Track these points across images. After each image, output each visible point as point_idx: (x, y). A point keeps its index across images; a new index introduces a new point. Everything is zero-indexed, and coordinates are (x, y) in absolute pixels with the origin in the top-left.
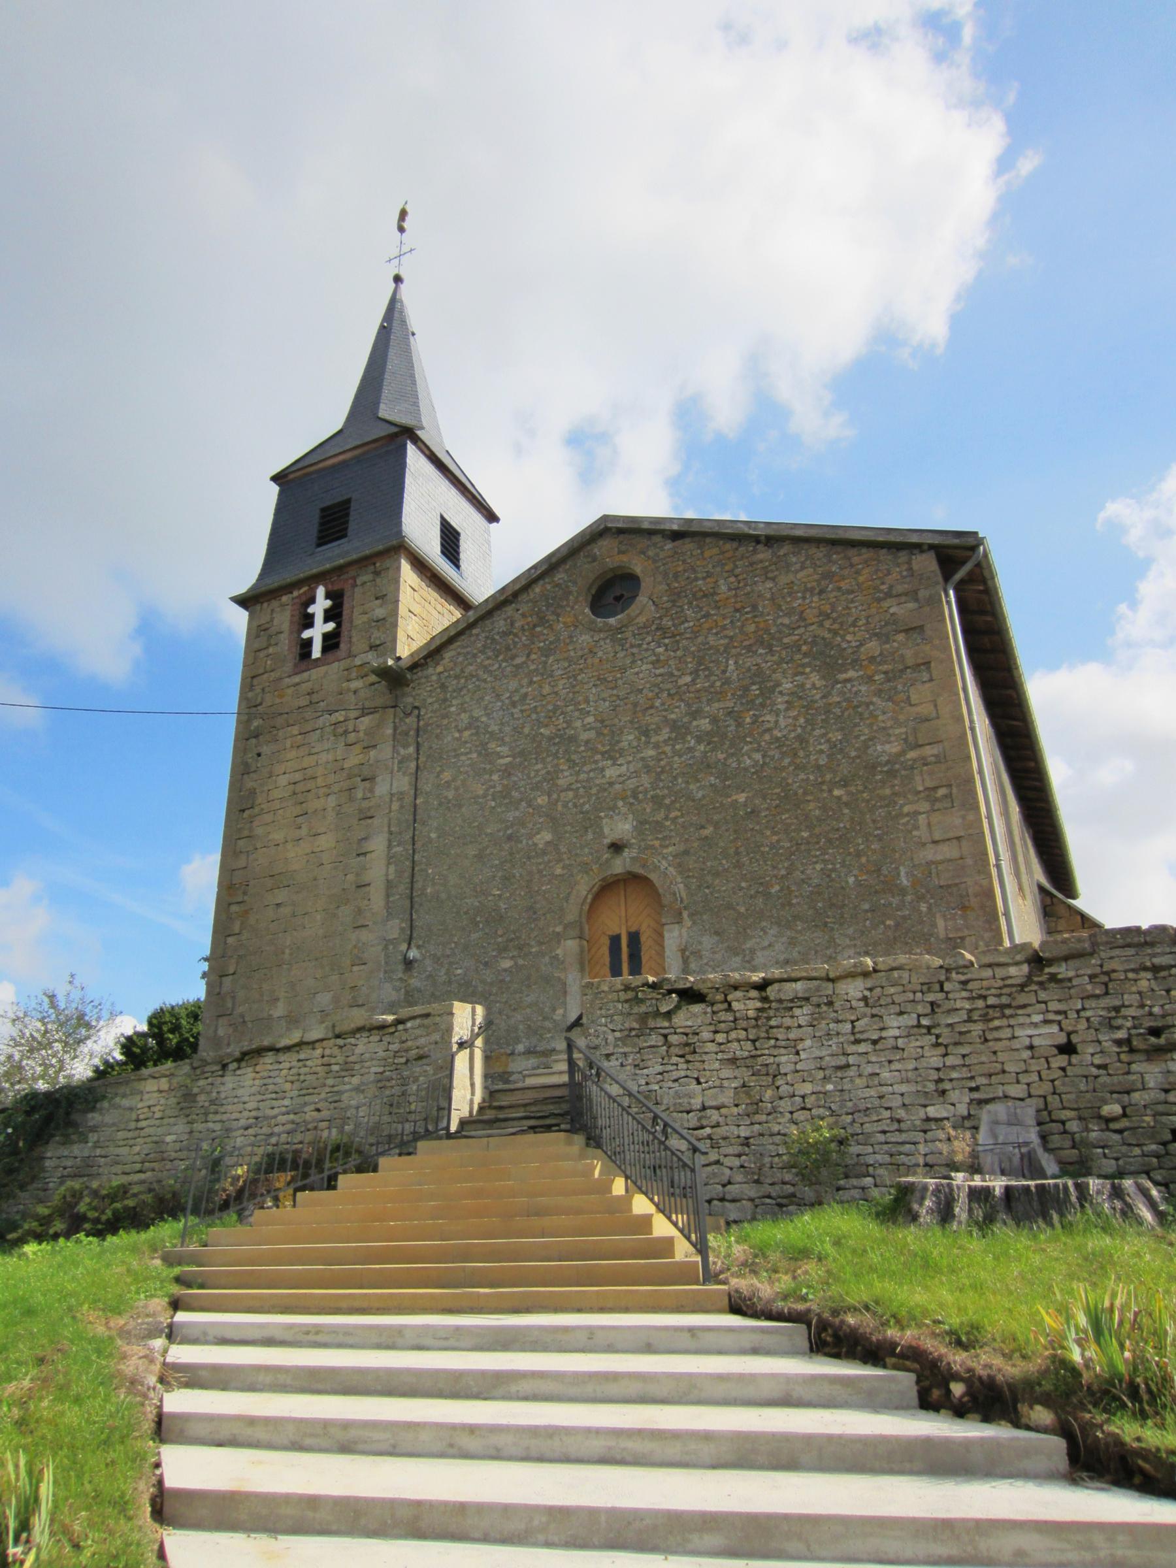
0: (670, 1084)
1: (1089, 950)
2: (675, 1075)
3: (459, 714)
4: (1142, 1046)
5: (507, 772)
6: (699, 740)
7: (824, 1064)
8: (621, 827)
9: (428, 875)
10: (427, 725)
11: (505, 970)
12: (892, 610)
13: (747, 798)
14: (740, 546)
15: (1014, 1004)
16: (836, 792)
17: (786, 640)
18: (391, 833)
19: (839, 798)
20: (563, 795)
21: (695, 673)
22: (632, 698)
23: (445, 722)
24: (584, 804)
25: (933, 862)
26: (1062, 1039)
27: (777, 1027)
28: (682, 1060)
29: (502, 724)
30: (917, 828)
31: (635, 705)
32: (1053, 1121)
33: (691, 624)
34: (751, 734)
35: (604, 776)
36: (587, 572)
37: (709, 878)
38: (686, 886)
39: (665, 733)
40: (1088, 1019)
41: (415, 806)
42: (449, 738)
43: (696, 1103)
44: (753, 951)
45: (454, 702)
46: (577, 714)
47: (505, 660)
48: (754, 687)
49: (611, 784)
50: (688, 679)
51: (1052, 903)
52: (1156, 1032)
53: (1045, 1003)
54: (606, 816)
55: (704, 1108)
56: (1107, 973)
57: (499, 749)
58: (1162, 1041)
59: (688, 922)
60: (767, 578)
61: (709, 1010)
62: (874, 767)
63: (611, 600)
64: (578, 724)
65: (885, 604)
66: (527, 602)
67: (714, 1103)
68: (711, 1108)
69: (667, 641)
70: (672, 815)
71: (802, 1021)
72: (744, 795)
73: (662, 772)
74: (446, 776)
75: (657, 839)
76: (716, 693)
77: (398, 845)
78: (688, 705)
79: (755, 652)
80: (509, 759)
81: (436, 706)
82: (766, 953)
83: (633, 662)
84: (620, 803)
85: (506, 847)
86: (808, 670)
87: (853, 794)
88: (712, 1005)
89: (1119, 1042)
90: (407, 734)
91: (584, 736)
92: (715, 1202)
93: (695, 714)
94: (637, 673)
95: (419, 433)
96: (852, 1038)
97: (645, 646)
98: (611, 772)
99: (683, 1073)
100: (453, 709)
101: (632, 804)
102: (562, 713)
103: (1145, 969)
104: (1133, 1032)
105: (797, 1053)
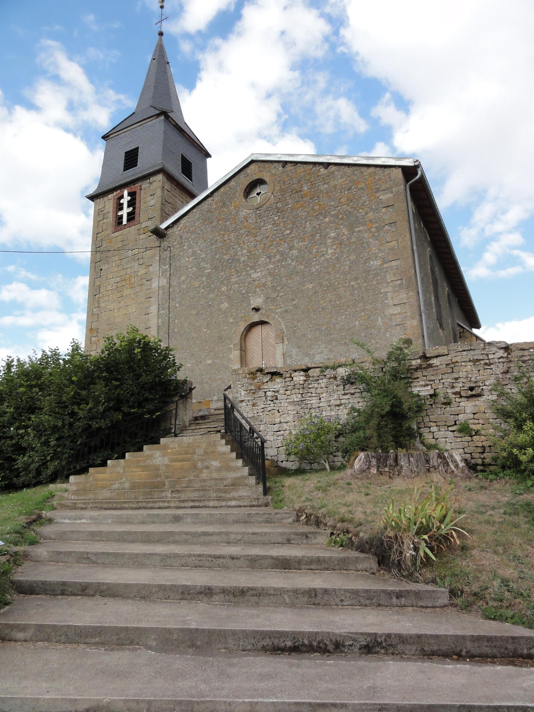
0: (267, 413)
1: (447, 353)
2: (269, 409)
3: (188, 250)
4: (465, 395)
5: (209, 275)
6: (293, 260)
7: (331, 404)
8: (257, 301)
9: (175, 323)
10: (174, 255)
11: (209, 364)
12: (380, 198)
13: (313, 286)
14: (313, 167)
15: (413, 377)
16: (352, 283)
17: (332, 213)
18: (159, 305)
19: (353, 286)
20: (233, 286)
21: (292, 229)
22: (264, 242)
23: (182, 253)
24: (242, 290)
25: (393, 314)
26: (432, 392)
27: (312, 388)
28: (272, 402)
29: (207, 254)
30: (387, 299)
31: (265, 244)
32: (425, 427)
33: (290, 206)
34: (315, 257)
35: (251, 277)
36: (244, 181)
37: (295, 323)
38: (286, 326)
39: (278, 257)
40: (443, 383)
41: (169, 291)
42: (184, 261)
43: (278, 420)
44: (314, 355)
45: (186, 244)
46: (239, 249)
47: (208, 224)
48: (317, 235)
49: (254, 281)
50: (288, 232)
51: (463, 332)
52: (471, 389)
53: (426, 376)
54: (252, 296)
55: (281, 423)
56: (453, 363)
57: (205, 266)
58: (474, 392)
59: (286, 342)
60: (325, 183)
61: (284, 381)
62: (369, 271)
63: (255, 195)
64: (240, 253)
65: (377, 195)
66: (219, 196)
67: (285, 421)
68: (284, 422)
69: (279, 214)
70: (281, 294)
71: (323, 385)
72: (312, 285)
73: (276, 275)
74: (183, 278)
75: (273, 305)
76: (301, 238)
77: (163, 310)
78: (288, 244)
79: (318, 219)
80: (210, 270)
81: (178, 246)
82: (319, 355)
83: (265, 224)
84: (258, 290)
85: (209, 310)
86: (341, 227)
87: (359, 284)
88: (285, 379)
89: (455, 393)
90: (165, 259)
91: (242, 259)
92: (284, 462)
93: (291, 248)
94: (266, 229)
95: (170, 114)
96: (343, 392)
97: (270, 217)
98: (255, 275)
99: (272, 408)
100: (185, 247)
101: (263, 290)
102: (233, 249)
103: (470, 361)
104: (462, 388)
105: (320, 399)
